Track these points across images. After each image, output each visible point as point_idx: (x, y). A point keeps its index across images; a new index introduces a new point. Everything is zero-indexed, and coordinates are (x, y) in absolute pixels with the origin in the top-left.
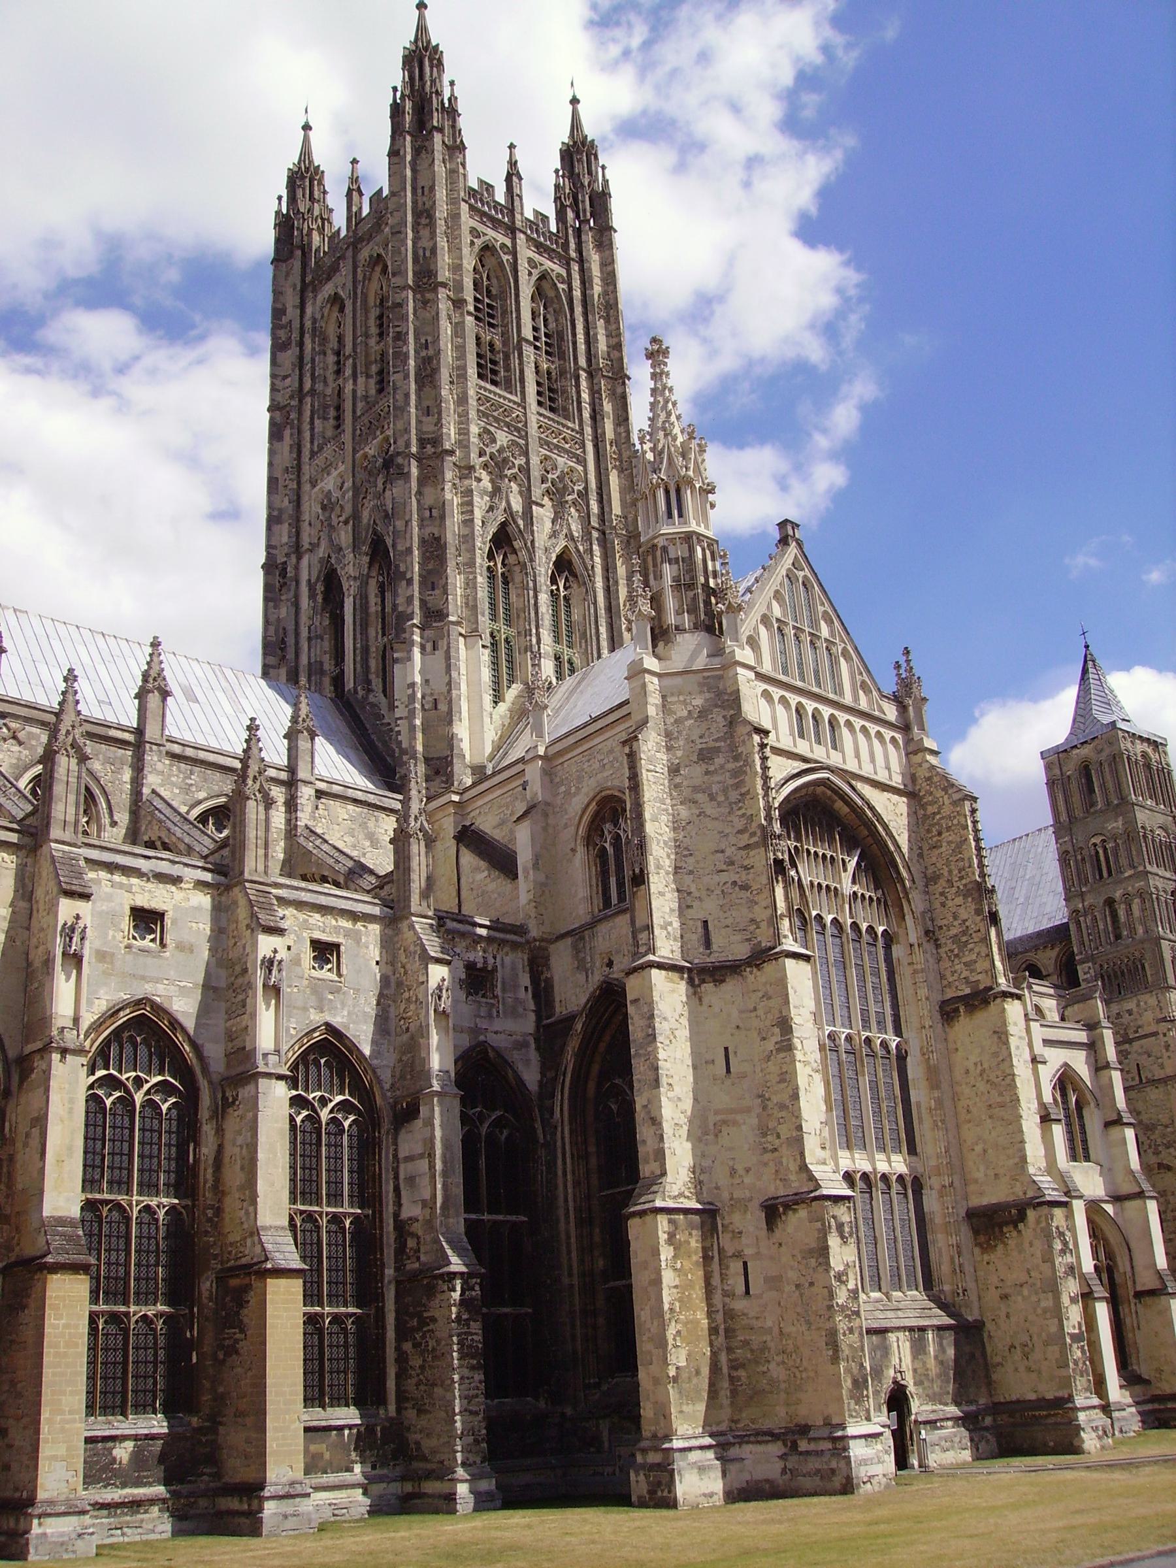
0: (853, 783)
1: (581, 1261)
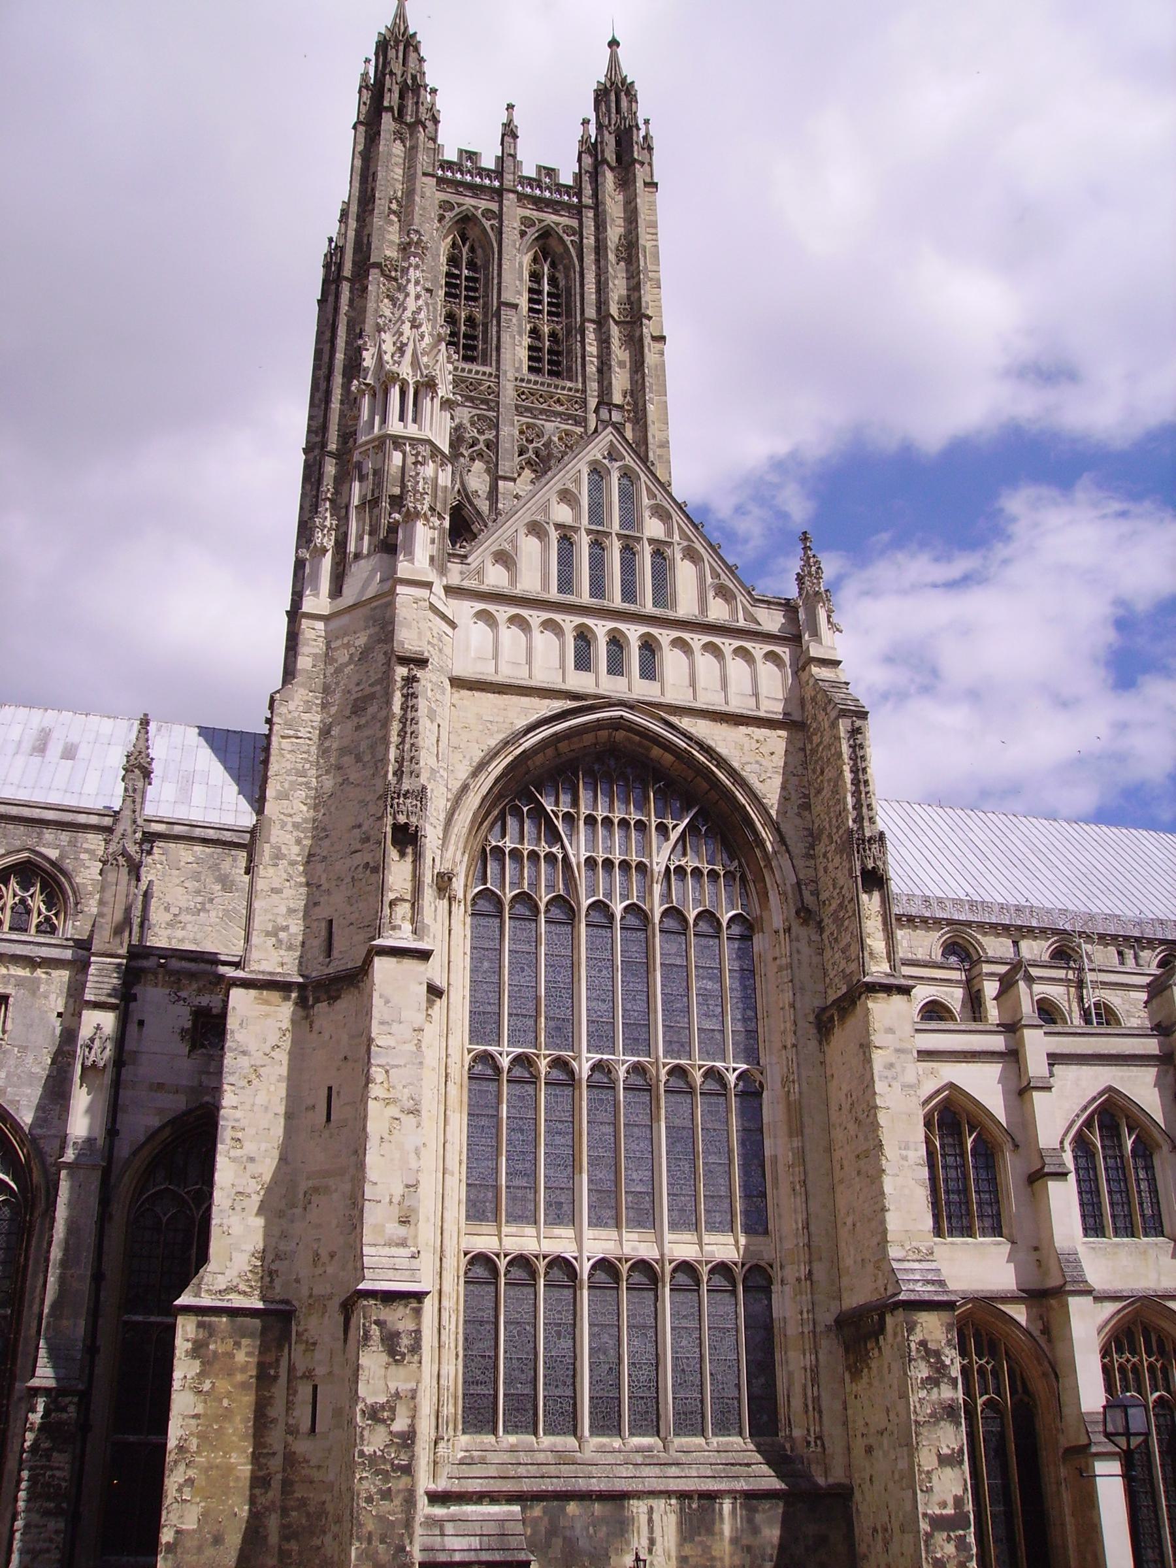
0: (674, 719)
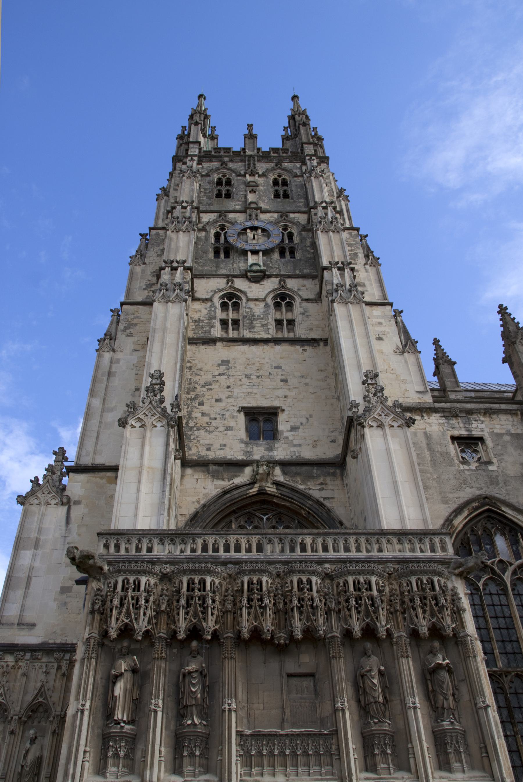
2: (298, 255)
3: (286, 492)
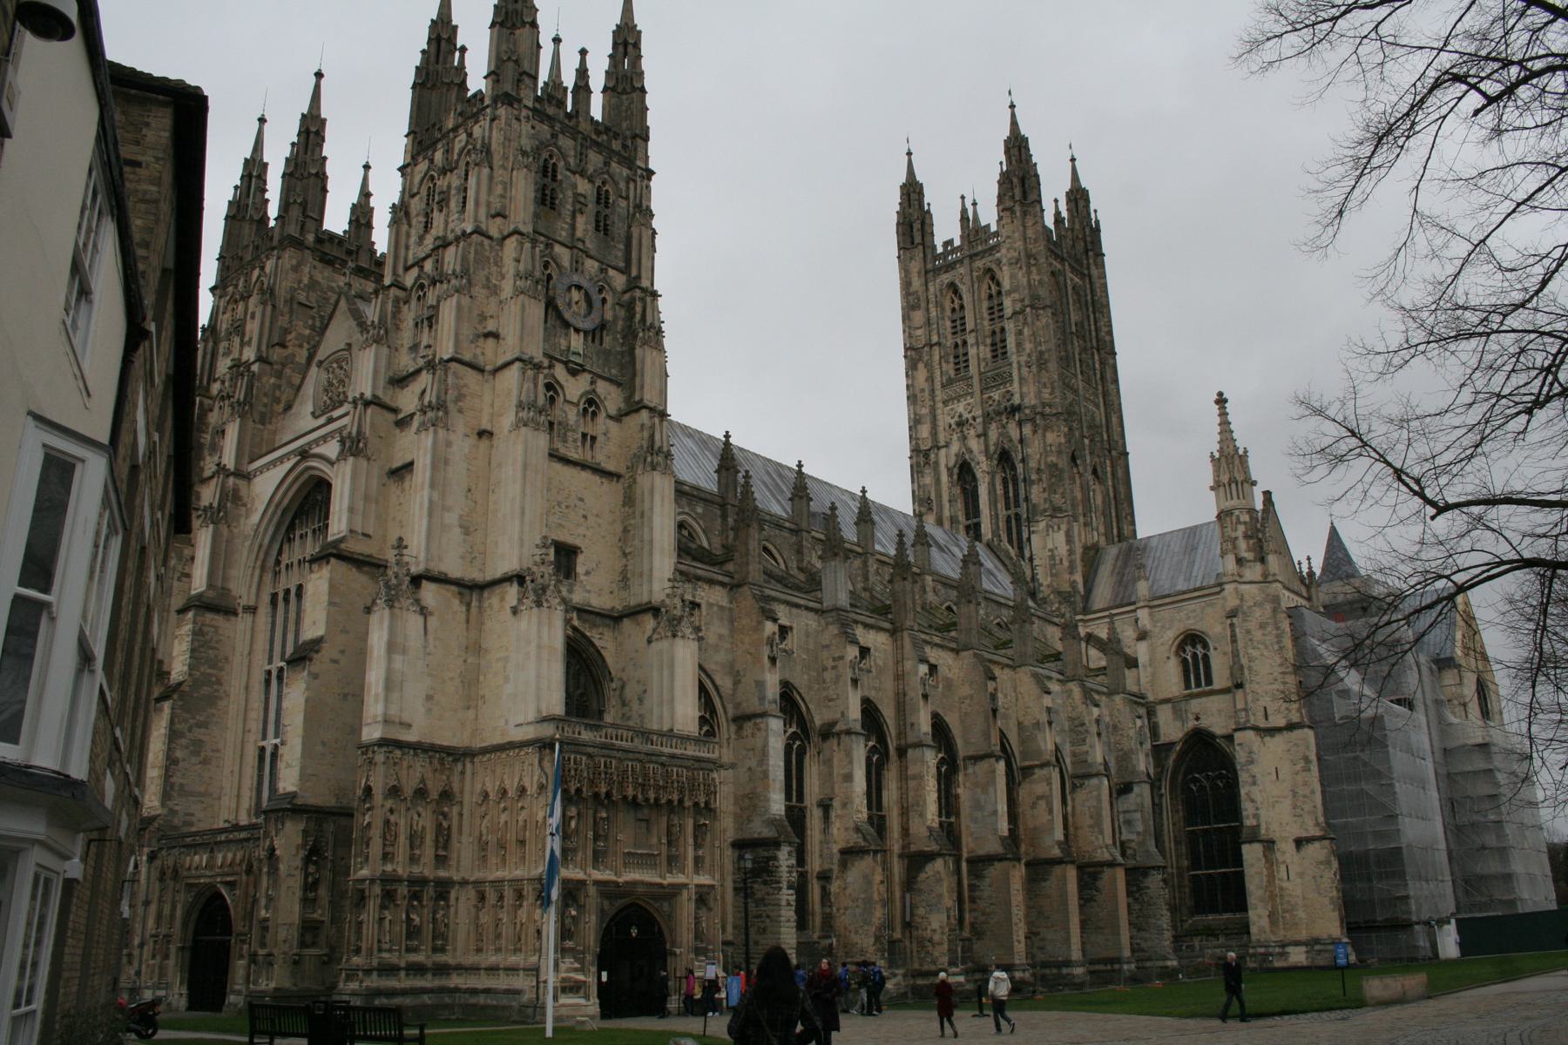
1: (1177, 861)
2: (607, 340)
3: (578, 636)
